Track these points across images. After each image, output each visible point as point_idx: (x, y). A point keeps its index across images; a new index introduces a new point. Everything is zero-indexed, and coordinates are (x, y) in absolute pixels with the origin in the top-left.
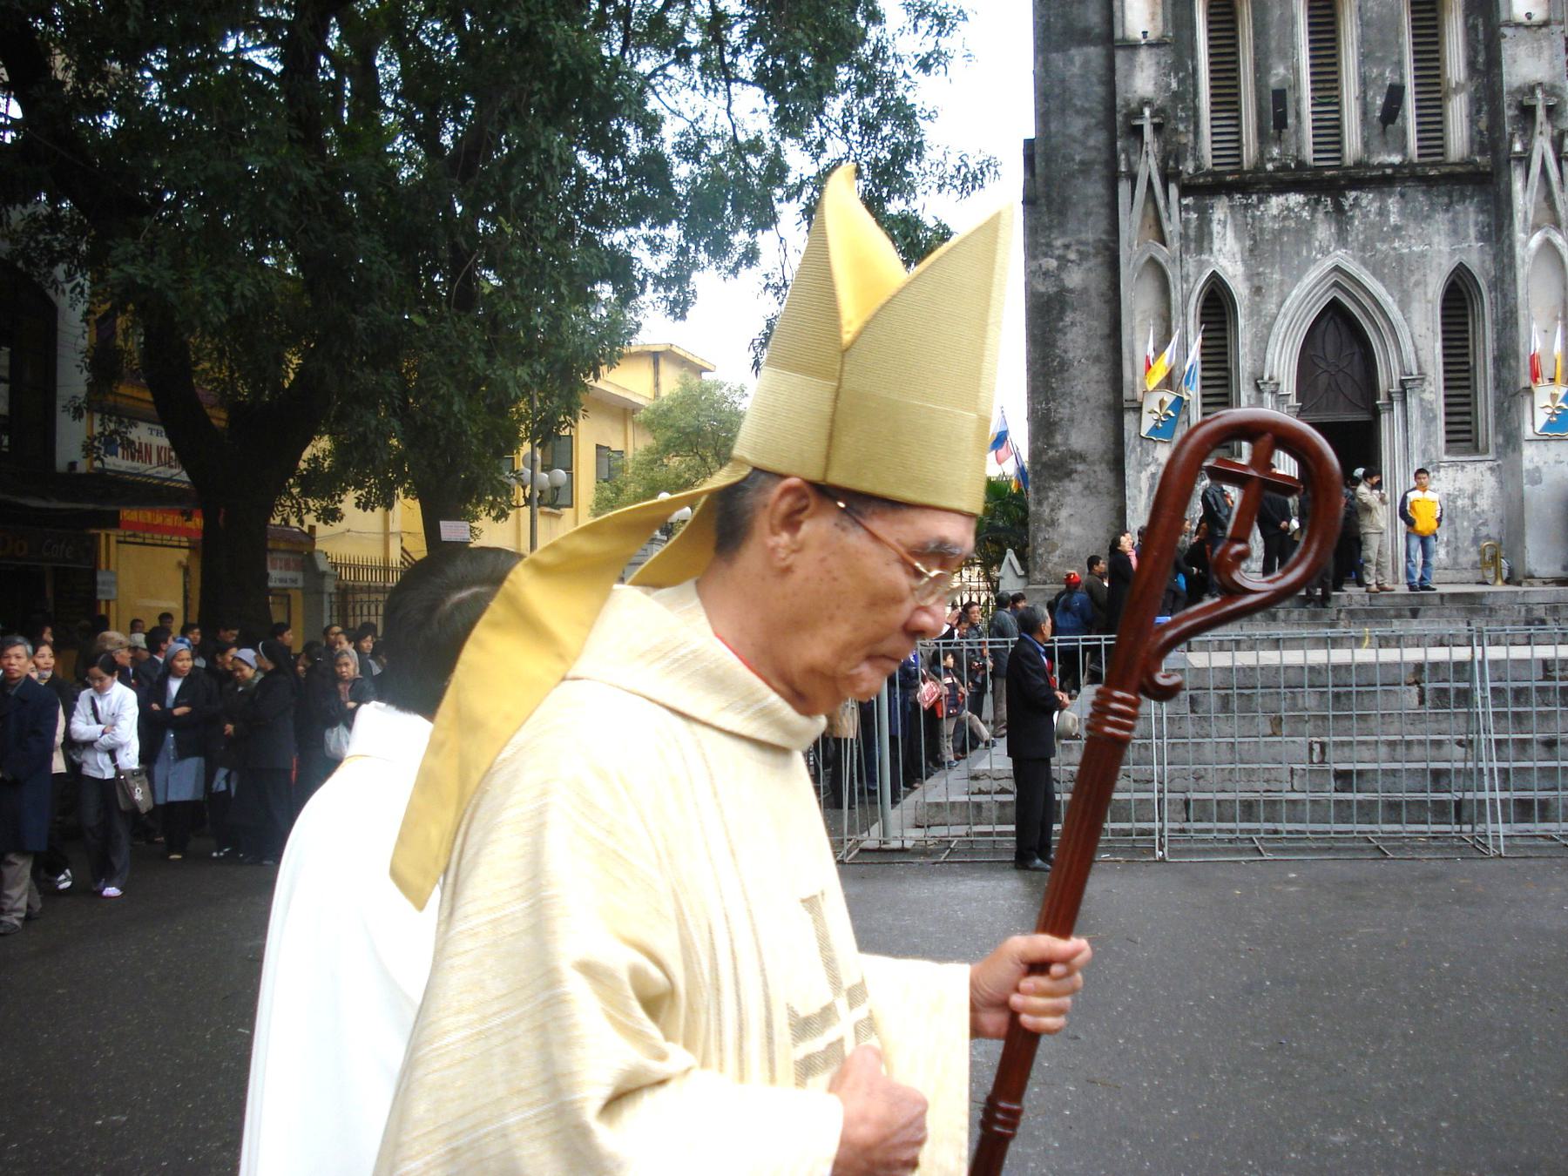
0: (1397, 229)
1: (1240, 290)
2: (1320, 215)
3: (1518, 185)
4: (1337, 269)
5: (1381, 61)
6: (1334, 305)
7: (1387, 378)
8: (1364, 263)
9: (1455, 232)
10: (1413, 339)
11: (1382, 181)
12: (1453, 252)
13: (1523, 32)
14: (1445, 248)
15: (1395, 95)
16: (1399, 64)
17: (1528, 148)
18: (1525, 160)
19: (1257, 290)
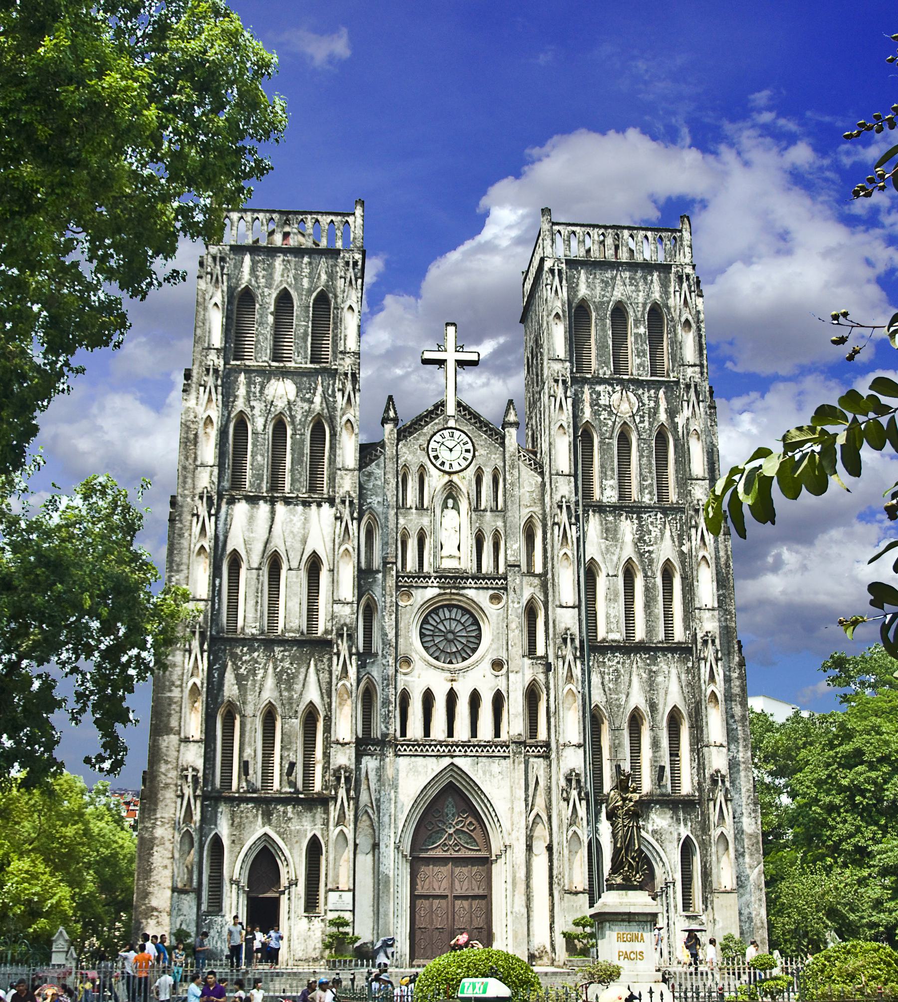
0: (290, 819)
1: (226, 842)
2: (260, 812)
3: (332, 808)
4: (265, 834)
5: (289, 749)
6: (265, 846)
8: (278, 833)
9: (313, 821)
11: (285, 801)
12: (312, 830)
13: (339, 746)
14: (309, 828)
17: (336, 793)
18: (335, 799)
19: (233, 842)
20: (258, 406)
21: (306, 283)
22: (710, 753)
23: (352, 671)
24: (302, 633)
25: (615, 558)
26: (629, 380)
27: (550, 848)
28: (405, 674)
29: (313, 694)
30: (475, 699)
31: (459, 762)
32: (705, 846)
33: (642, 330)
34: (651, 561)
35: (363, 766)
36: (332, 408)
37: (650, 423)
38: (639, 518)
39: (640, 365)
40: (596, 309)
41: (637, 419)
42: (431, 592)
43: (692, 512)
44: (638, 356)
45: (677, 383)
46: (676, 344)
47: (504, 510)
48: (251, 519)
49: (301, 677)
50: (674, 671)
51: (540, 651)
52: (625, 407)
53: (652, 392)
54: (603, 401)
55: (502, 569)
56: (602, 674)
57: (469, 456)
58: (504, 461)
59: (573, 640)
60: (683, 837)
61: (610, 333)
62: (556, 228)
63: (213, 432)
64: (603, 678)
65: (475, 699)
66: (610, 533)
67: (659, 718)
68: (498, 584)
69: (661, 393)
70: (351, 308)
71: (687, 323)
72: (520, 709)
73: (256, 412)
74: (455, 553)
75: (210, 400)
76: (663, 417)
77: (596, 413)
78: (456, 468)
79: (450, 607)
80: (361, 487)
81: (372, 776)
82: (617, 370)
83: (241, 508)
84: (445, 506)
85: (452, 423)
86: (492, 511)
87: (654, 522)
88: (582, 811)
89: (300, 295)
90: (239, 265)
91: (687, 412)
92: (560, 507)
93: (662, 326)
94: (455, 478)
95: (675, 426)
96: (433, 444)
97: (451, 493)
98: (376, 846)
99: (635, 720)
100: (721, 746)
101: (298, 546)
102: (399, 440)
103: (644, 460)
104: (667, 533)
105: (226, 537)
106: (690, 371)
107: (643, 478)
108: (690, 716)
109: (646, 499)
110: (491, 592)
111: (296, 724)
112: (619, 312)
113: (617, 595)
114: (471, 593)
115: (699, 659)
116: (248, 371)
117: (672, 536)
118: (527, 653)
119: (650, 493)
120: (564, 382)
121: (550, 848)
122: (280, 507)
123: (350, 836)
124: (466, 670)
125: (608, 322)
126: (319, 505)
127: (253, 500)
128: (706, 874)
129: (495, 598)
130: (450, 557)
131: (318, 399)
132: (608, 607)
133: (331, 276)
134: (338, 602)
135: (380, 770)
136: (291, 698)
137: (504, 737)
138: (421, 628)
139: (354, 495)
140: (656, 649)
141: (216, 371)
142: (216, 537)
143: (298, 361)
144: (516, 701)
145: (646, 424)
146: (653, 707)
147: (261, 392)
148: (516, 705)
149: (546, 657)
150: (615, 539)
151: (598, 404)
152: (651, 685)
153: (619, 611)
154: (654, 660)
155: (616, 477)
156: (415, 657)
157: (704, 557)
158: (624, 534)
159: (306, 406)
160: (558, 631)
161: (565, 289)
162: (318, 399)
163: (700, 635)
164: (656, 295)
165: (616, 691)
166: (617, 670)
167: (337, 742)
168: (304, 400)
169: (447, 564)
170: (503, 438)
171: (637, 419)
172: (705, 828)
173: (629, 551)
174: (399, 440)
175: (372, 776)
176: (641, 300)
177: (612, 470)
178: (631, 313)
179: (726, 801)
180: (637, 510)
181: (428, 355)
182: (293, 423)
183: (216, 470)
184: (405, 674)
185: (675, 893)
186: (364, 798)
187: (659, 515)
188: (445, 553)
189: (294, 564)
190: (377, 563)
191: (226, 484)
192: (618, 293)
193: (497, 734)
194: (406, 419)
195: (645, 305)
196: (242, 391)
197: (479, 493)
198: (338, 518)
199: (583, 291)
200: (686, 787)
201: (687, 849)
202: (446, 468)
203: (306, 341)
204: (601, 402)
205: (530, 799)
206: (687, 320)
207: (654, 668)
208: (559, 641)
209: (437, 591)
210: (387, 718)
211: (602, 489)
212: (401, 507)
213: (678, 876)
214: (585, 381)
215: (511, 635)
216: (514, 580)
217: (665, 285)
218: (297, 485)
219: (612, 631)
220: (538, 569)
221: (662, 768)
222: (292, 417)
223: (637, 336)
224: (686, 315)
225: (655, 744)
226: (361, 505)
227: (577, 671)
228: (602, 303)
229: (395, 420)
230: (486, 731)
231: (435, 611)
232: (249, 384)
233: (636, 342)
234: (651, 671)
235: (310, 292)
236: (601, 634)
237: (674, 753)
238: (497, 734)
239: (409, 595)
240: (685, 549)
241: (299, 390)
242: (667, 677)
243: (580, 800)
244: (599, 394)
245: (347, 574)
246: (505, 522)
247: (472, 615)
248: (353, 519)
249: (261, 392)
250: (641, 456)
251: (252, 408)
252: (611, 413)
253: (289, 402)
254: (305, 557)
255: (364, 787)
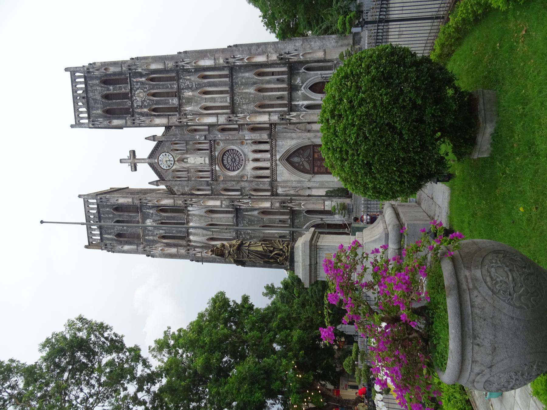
7: (321, 222)
10: (317, 219)
15: (280, 221)
16: (276, 219)
18: (291, 207)
20: (156, 232)
21: (111, 216)
22: (271, 60)
23: (245, 201)
24: (234, 217)
25: (199, 99)
26: (131, 93)
27: (309, 123)
28: (247, 178)
29: (256, 213)
30: (255, 151)
31: (278, 157)
32: (307, 62)
33: (111, 88)
34: (199, 84)
35: (281, 193)
36: (152, 207)
37: (147, 84)
38: (183, 89)
39: (124, 88)
40: (106, 106)
41: (145, 90)
42: (217, 168)
43: (178, 68)
44: (121, 90)
45: (129, 73)
46: (114, 74)
47: (186, 141)
48: (195, 234)
49: (249, 217)
50: (240, 75)
51: (237, 126)
52: (141, 95)
53: (134, 84)
54: (141, 104)
55: (208, 142)
56: (243, 104)
57: (168, 154)
58: (168, 141)
59: (230, 117)
60: (304, 70)
61: (114, 101)
62: (77, 122)
63: (166, 249)
64: (244, 104)
65: (255, 151)
66: (189, 101)
67: (259, 81)
68: (213, 144)
69: (134, 80)
70: (117, 200)
71: (105, 69)
72: (258, 135)
73: (158, 233)
74: (203, 158)
75: (155, 250)
76: (143, 79)
77: (145, 107)
78: (172, 159)
79: (223, 160)
80: (182, 194)
81: (284, 189)
82: (128, 98)
83: (191, 237)
84: (187, 162)
85: (156, 161)
86: (186, 145)
87: (184, 83)
88: (294, 114)
89: (115, 218)
90: (108, 239)
91: (140, 70)
92: (180, 122)
93: (109, 79)
94: (176, 159)
95: (147, 74)
96: (165, 168)
97: (182, 160)
98: (309, 188)
99: (260, 90)
100: (268, 56)
101: (203, 218)
102: (164, 180)
103: (161, 87)
104: (188, 77)
105: (202, 243)
106: (124, 68)
107: (168, 87)
108: (257, 68)
109: (176, 86)
110: (216, 146)
111: (266, 218)
112: (107, 97)
113: (212, 98)
114: (217, 154)
115: (234, 65)
116: (144, 236)
117: (189, 76)
118: (237, 132)
119: (173, 84)
120: (134, 120)
121: (309, 123)
122: (191, 224)
123: (305, 202)
124: (245, 155)
125: (110, 102)
126: (189, 211)
127: (188, 234)
128: (318, 61)
129: (218, 144)
130: (205, 161)
131: (151, 211)
132: (217, 102)
133: (108, 206)
134: (221, 206)
135: (282, 187)
136: (257, 221)
137: (268, 140)
138: (231, 171)
139: (183, 200)
140: (232, 82)
141: (144, 248)
142: (202, 247)
143: (139, 217)
144: (255, 137)
145: (147, 86)
146: (254, 83)
147: (151, 231)
148: (256, 136)
149: (239, 125)
150: (192, 99)
151: (142, 106)
152: (246, 85)
153: (219, 97)
154: (236, 83)
155: (168, 98)
156: (241, 173)
157: (195, 63)
158: (189, 95)
159: (154, 215)
160: (227, 123)
161: (99, 120)
162: (151, 211)
163: (225, 65)
164: (97, 82)
165: (249, 99)
166: (241, 98)
167: (271, 206)
168: (152, 217)
169: (207, 161)
170: (160, 141)
171: (145, 90)
172: (301, 63)
173: (196, 93)
174: (164, 180)
175: (284, 189)
176: (100, 88)
177: (166, 100)
178: (105, 92)
179: (289, 53)
180: (179, 90)
181: (133, 169)
182: (160, 220)
183: (179, 248)
184: (247, 178)
185: (325, 74)
186: (292, 192)
187: (181, 81)
188: (203, 162)
189: (210, 219)
190: (209, 188)
191: (184, 243)
192: (98, 97)
193: (267, 142)
194: (157, 178)
195: (102, 87)
196: (151, 238)
197: (181, 150)
198: (192, 205)
199: (99, 112)
200: (285, 69)
201: (308, 69)
202: (173, 162)
203: (131, 216)
204: (141, 104)
205: (291, 131)
206: (105, 69)
207: (240, 83)
208: (231, 123)
209: (217, 166)
210: (264, 183)
211: (173, 104)
212: (189, 179)
213: (319, 72)
214: (133, 111)
215: (231, 138)
216: (211, 137)
217: (92, 78)
218: (182, 218)
219: (226, 101)
220: (207, 127)
221: (278, 80)
222: (158, 220)
223: (114, 89)
224: (103, 70)
225: (269, 82)
226: (189, 195)
227: (241, 115)
228: (103, 104)
229: (157, 181)
230: (267, 147)
231: (224, 166)
232: (149, 235)
233: (116, 90)
234: (241, 84)
235: (114, 214)
236: (227, 104)
237: (273, 74)
238: (267, 142)
239: (219, 176)
240: (193, 71)
241: (148, 218)
242: (243, 77)
243: (290, 115)
244: (137, 106)
245: (211, 203)
246: (190, 141)
247: (225, 152)
248: (191, 200)
249: (151, 231)
250: (160, 88)
251: (157, 234)
252: (144, 101)
253: (153, 221)
254: (207, 215)
255: (288, 192)
